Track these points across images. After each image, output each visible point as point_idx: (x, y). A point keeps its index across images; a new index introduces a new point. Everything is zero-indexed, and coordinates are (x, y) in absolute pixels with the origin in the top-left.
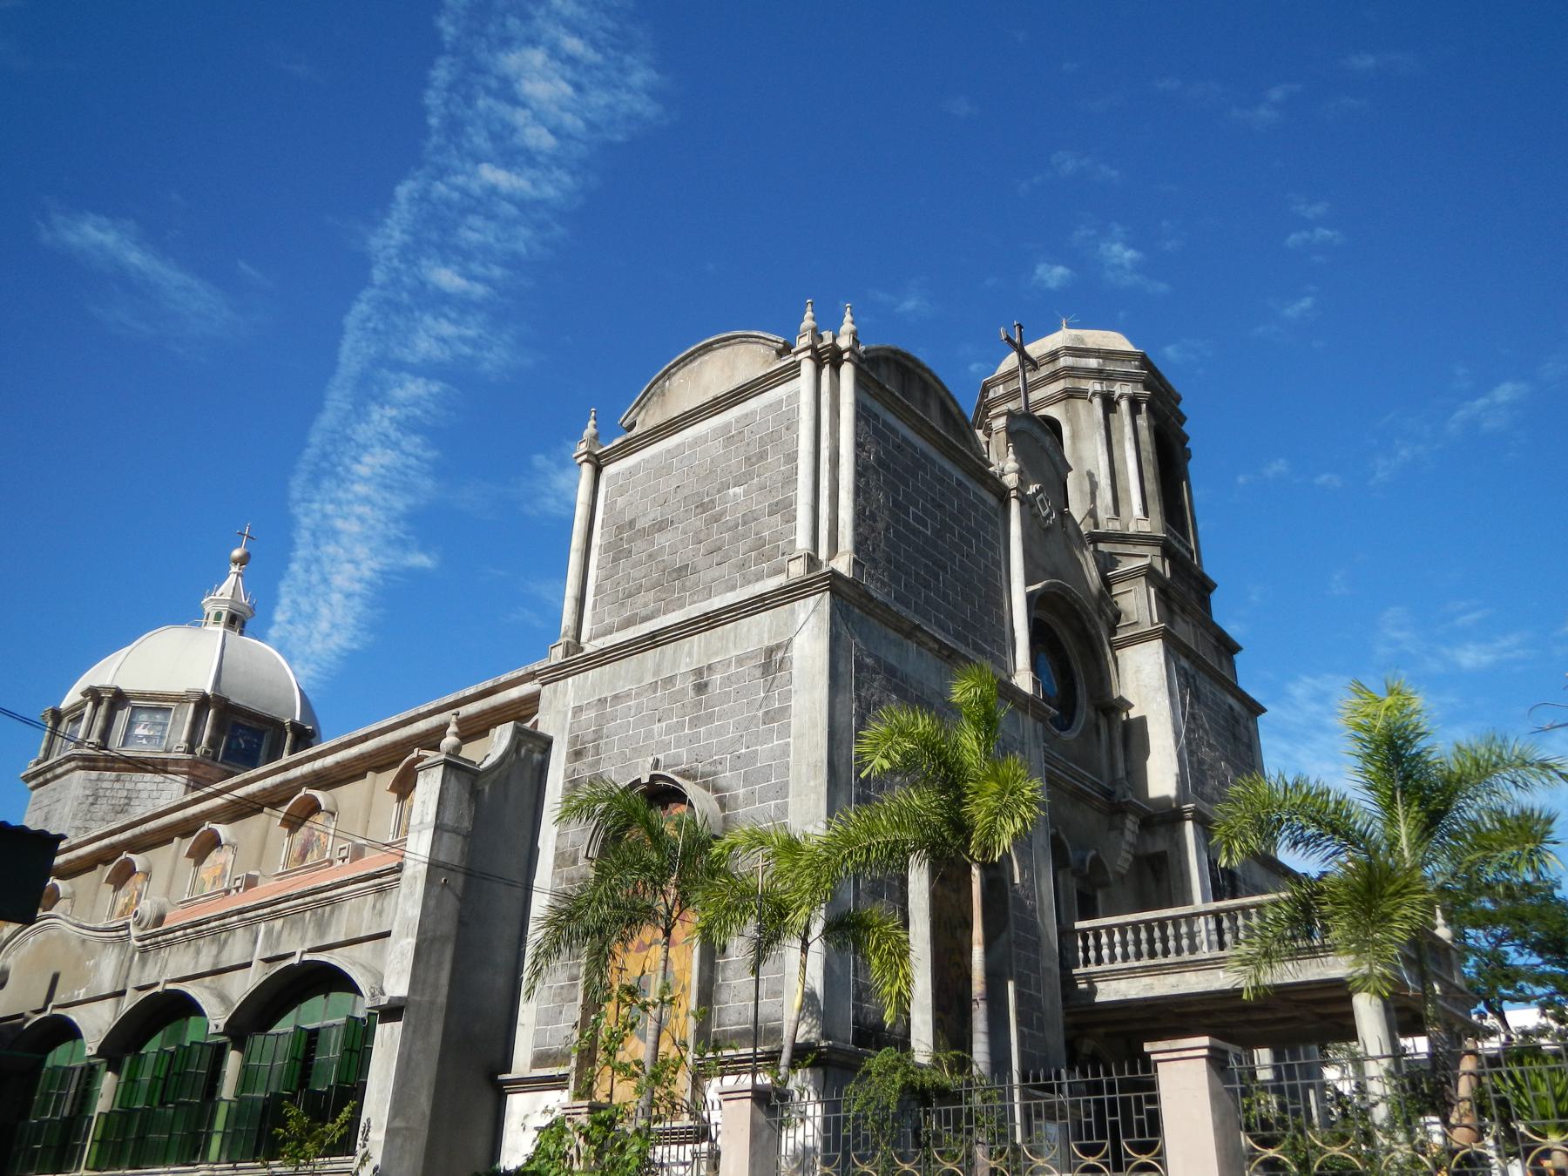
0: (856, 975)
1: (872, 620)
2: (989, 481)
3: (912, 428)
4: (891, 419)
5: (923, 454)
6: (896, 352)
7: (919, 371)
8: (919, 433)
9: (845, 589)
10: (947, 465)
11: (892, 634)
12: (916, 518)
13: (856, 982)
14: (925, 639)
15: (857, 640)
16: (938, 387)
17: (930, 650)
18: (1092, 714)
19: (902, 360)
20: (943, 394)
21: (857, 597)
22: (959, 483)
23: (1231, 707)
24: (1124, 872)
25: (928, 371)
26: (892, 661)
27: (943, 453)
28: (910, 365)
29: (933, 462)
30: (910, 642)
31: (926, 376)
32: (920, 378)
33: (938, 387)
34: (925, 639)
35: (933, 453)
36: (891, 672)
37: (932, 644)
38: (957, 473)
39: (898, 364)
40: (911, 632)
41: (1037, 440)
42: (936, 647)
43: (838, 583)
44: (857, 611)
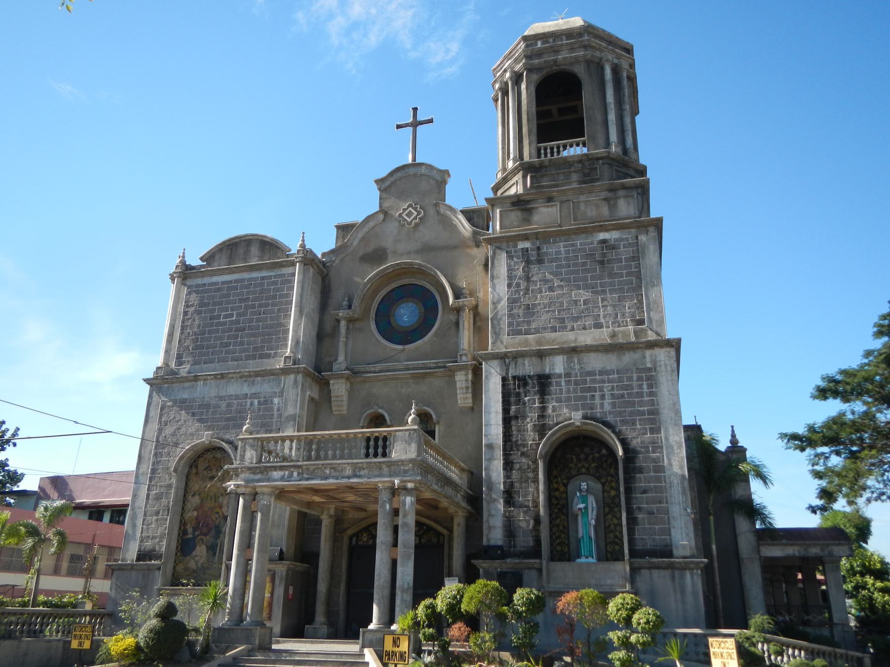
0: (142, 533)
1: (174, 385)
2: (284, 263)
3: (229, 274)
4: (215, 279)
5: (236, 281)
6: (224, 243)
7: (243, 239)
8: (234, 273)
9: (155, 381)
10: (255, 275)
11: (187, 384)
12: (226, 317)
13: (141, 537)
14: (204, 377)
15: (164, 398)
16: (255, 237)
17: (212, 379)
18: (453, 318)
19: (232, 242)
20: (260, 238)
21: (161, 381)
22: (263, 278)
23: (604, 241)
24: (471, 405)
25: (246, 235)
26: (185, 396)
27: (251, 271)
28: (236, 240)
29: (243, 280)
30: (199, 383)
31: (248, 238)
32: (245, 241)
33: (255, 237)
34: (206, 377)
35: (246, 275)
36: (183, 401)
37: (209, 377)
38: (265, 274)
39: (228, 246)
40: (196, 379)
41: (415, 175)
42: (213, 377)
43: (151, 381)
44: (166, 385)
